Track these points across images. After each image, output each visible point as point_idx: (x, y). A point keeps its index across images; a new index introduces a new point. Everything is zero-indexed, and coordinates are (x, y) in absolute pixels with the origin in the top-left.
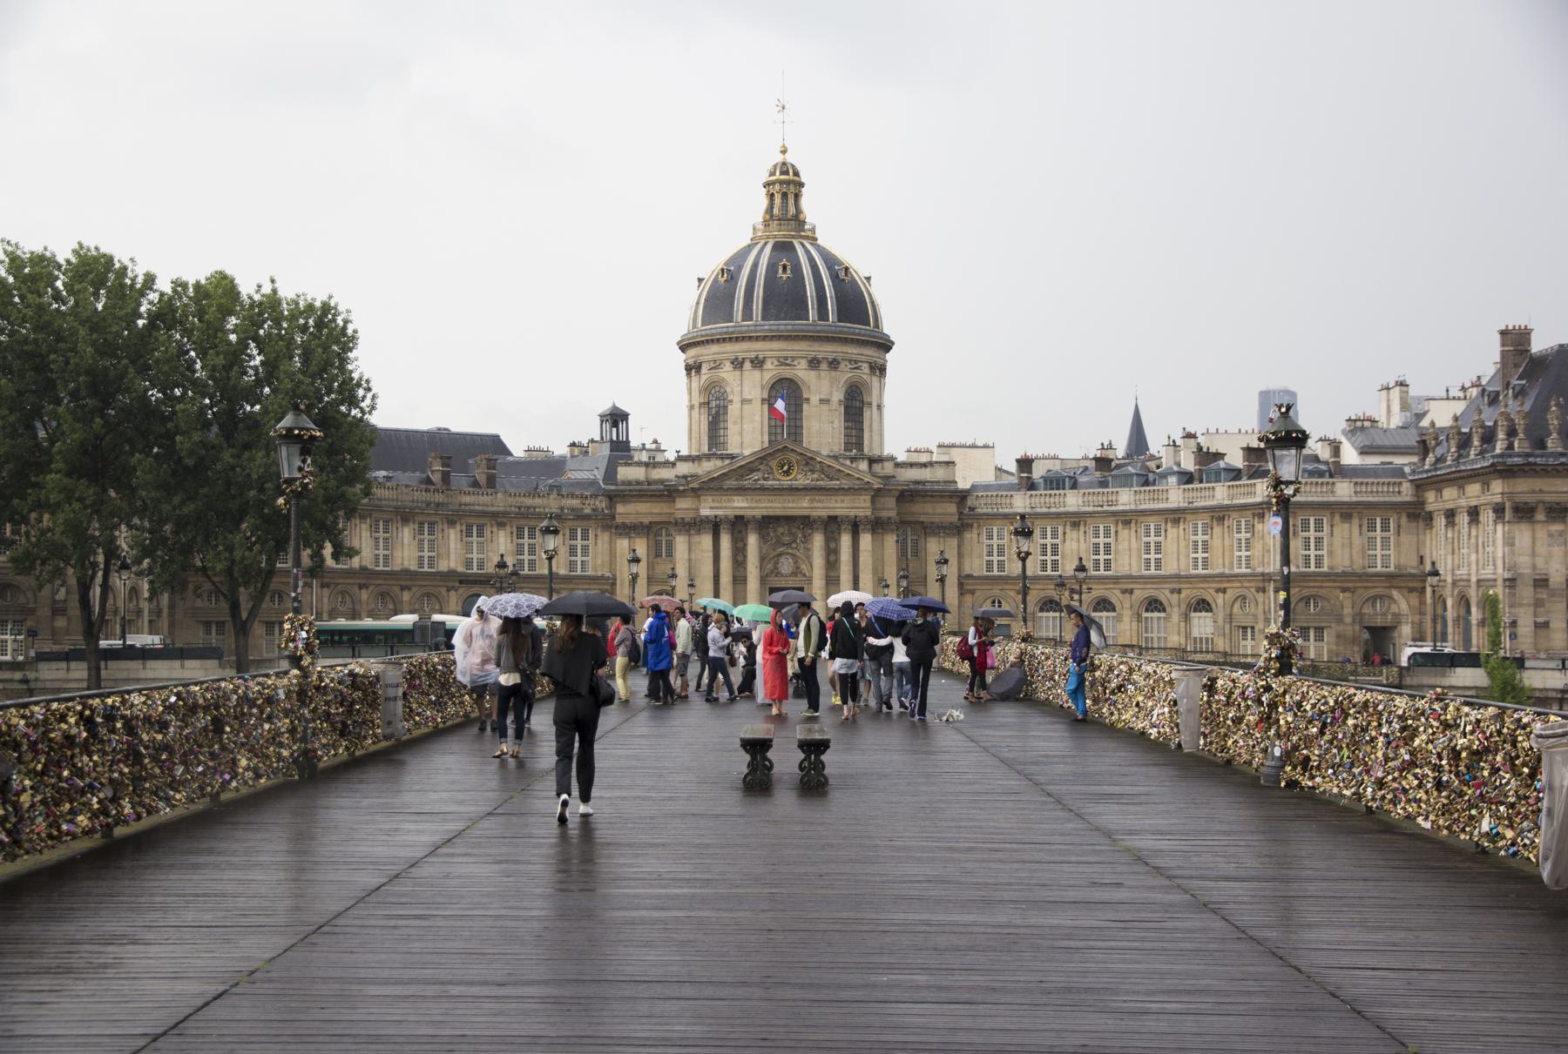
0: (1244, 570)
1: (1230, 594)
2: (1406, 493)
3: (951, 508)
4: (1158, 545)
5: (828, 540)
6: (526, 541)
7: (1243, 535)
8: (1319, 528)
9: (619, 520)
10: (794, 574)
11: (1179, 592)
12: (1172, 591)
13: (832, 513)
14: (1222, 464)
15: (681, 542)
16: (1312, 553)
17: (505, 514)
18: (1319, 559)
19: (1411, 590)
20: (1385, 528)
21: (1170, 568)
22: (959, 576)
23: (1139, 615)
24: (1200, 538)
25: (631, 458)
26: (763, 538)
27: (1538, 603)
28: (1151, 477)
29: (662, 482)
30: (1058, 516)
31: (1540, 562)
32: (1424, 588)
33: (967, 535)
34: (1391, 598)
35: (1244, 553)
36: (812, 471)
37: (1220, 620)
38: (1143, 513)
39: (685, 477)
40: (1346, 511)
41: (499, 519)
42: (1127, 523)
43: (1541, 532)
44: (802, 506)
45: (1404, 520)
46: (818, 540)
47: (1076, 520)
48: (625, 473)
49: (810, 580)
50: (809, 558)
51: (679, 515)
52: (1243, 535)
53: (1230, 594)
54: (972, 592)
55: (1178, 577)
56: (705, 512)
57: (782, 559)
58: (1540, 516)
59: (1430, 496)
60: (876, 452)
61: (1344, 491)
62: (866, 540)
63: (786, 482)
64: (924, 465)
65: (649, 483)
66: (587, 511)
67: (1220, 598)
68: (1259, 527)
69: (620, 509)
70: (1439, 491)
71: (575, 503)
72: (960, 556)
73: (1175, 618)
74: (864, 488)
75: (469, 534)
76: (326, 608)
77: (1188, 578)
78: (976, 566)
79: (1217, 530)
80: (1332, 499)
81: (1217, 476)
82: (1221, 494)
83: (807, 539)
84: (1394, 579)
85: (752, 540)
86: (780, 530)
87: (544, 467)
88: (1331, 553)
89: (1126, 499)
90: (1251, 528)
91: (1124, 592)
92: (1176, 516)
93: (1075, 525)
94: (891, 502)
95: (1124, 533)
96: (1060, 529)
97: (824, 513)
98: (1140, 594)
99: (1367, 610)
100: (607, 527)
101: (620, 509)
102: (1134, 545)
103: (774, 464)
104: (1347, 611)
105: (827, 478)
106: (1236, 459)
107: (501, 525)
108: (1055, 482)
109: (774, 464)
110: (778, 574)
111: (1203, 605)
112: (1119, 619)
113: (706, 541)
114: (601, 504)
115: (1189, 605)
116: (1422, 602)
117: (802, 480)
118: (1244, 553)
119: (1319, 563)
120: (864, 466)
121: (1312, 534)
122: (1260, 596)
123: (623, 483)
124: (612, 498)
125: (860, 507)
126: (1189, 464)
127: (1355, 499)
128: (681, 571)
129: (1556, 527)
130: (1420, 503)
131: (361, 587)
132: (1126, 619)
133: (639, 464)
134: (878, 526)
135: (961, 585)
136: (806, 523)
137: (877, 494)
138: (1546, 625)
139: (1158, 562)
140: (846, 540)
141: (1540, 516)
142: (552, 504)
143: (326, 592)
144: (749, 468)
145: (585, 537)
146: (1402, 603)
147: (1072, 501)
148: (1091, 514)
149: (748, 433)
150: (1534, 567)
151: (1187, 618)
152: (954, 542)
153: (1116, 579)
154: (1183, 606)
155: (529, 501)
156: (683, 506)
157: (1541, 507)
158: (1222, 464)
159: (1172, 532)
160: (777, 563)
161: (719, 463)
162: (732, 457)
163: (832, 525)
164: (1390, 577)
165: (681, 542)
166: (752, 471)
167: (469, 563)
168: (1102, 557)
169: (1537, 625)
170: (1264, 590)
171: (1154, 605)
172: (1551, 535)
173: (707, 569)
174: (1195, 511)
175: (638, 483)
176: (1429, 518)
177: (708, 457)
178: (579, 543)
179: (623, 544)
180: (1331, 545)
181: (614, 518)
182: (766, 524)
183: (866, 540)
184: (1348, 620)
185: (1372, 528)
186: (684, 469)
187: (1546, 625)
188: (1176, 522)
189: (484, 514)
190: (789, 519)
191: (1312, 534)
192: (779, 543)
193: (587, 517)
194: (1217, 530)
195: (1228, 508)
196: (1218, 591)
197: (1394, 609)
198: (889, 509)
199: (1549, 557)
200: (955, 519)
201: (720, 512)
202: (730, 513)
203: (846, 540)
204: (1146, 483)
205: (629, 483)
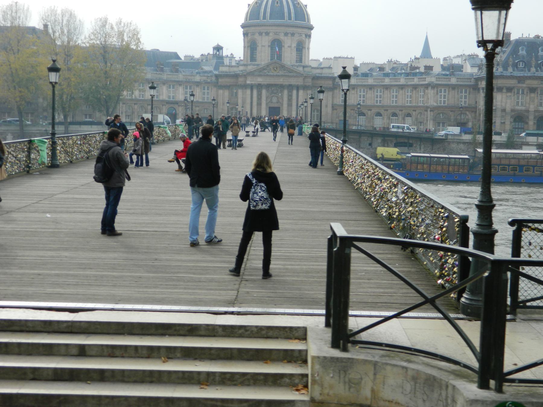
0: (421, 104)
1: (417, 112)
2: (472, 82)
3: (330, 82)
4: (396, 96)
5: (289, 92)
7: (422, 94)
8: (445, 92)
9: (219, 84)
10: (277, 103)
11: (402, 111)
12: (400, 110)
13: (290, 83)
14: (418, 71)
15: (240, 92)
16: (442, 99)
17: (182, 81)
18: (444, 102)
19: (472, 112)
20: (466, 92)
21: (400, 103)
22: (332, 104)
23: (389, 118)
24: (409, 94)
25: (223, 63)
26: (268, 91)
27: (502, 116)
28: (396, 74)
29: (234, 72)
30: (365, 86)
31: (503, 104)
32: (476, 111)
33: (335, 91)
34: (466, 114)
35: (422, 99)
36: (284, 70)
37: (414, 119)
38: (392, 86)
39: (242, 71)
40: (453, 87)
41: (180, 83)
42: (387, 89)
43: (504, 96)
44: (280, 81)
45: (471, 90)
46: (286, 92)
47: (371, 87)
48: (222, 69)
49: (282, 105)
50: (282, 97)
51: (239, 83)
52: (422, 94)
53: (417, 112)
54: (336, 109)
55: (402, 107)
56: (248, 82)
57: (273, 98)
58: (504, 91)
59: (479, 83)
60: (307, 64)
61: (453, 81)
62: (301, 92)
63: (275, 73)
64: (322, 68)
65: (230, 72)
66: (209, 81)
67: (414, 113)
68: (426, 91)
69: (220, 80)
70: (481, 81)
71: (205, 78)
72: (333, 98)
73: (400, 119)
74: (302, 75)
75: (170, 88)
76: (124, 110)
77: (405, 107)
79: (414, 92)
80: (449, 83)
81: (415, 74)
82: (416, 81)
83: (282, 92)
84: (466, 108)
85: (264, 92)
86: (273, 89)
87: (193, 64)
88: (448, 100)
89: (387, 81)
90: (424, 92)
91: (385, 110)
92: (402, 87)
93: (370, 89)
94: (310, 80)
95: (386, 92)
96: (366, 90)
97: (287, 83)
98: (390, 111)
99: (459, 117)
100: (215, 86)
101: (220, 80)
102: (389, 96)
103: (271, 67)
104: (452, 118)
105: (289, 71)
106: (422, 70)
107: (180, 85)
108: (365, 75)
109: (271, 67)
110: (272, 103)
111: (409, 115)
112: (383, 119)
113: (248, 92)
114: (214, 79)
115: (405, 115)
116: (476, 116)
117: (281, 73)
118: (422, 99)
119: (444, 103)
120: (301, 69)
121: (443, 94)
122: (426, 113)
123: (221, 72)
124: (217, 76)
125: (299, 81)
126: (408, 71)
127: (456, 83)
128: (240, 102)
129: (509, 94)
130: (477, 85)
131: (135, 104)
132: (385, 119)
133: (226, 66)
134: (305, 88)
135: (333, 107)
136: (282, 87)
137: (306, 77)
138: (504, 123)
139: (396, 102)
140: (295, 92)
141: (504, 91)
142: (198, 78)
143: (124, 105)
144: (263, 69)
145: (208, 89)
146: (470, 116)
147: (370, 81)
148: (376, 85)
149: (264, 56)
150: (502, 105)
151: (404, 119)
152: (331, 93)
153: (383, 107)
154: (403, 115)
155: (189, 77)
156: (241, 80)
157: (505, 88)
158: (418, 71)
159: (401, 92)
160: (271, 99)
161: (253, 67)
162: (258, 65)
163: (290, 87)
164: (466, 107)
165: (240, 92)
166: (264, 69)
167: (169, 97)
168: (379, 99)
169: (501, 123)
170: (427, 111)
171: (394, 115)
172: (507, 96)
173: (248, 101)
174: (408, 86)
175: (226, 72)
176: (479, 89)
177: (250, 65)
178: (206, 91)
179: (221, 91)
180: (448, 97)
181: (217, 83)
183: (301, 92)
184: (452, 120)
185: (462, 92)
186: (241, 68)
187: (504, 123)
188: (402, 89)
189: (175, 81)
190: (276, 85)
191: (443, 94)
193: (209, 83)
194: (414, 92)
195: (418, 85)
196: (413, 110)
197: (467, 117)
198: (309, 82)
199: (506, 103)
200: (332, 86)
201: (253, 83)
202: (256, 83)
203: (295, 92)
204: (395, 76)
205: (223, 72)
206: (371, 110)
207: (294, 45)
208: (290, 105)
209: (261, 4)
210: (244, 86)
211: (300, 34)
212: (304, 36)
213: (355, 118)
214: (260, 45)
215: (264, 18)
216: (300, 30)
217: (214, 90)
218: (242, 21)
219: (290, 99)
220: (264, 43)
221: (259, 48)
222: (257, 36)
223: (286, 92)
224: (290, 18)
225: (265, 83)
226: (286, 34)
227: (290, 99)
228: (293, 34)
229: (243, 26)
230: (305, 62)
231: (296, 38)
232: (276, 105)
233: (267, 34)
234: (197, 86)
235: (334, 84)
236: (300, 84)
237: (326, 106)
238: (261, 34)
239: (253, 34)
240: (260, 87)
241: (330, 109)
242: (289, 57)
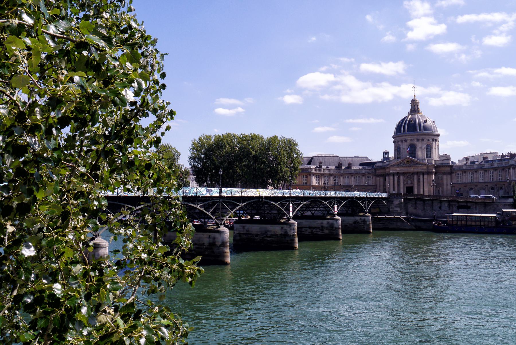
6: (358, 179)
21: (495, 180)
62: (426, 176)
78: (455, 181)
83: (413, 176)
89: (486, 166)
98: (489, 186)
101: (377, 171)
107: (352, 176)
113: (391, 178)
114: (374, 171)
140: (421, 177)
151: (498, 191)
152: (450, 176)
171: (493, 188)
173: (392, 183)
179: (378, 178)
182: (403, 174)
183: (426, 176)
190: (409, 173)
192: (408, 177)
193: (370, 173)
203: (421, 177)
206: (477, 186)
207: (424, 146)
208: (419, 184)
209: (402, 123)
210: (389, 174)
211: (428, 140)
212: (431, 140)
213: (468, 192)
214: (402, 148)
215: (404, 131)
216: (428, 137)
217: (374, 178)
218: (393, 134)
219: (419, 181)
220: (404, 146)
221: (402, 150)
222: (400, 143)
223: (416, 177)
224: (420, 130)
225: (402, 171)
226: (418, 140)
227: (419, 181)
228: (423, 140)
229: (393, 138)
230: (435, 157)
231: (425, 141)
232: (411, 185)
233: (406, 141)
234: (363, 176)
235: (451, 170)
236: (424, 171)
237: (447, 185)
238: (402, 141)
239: (398, 142)
240: (398, 174)
241: (449, 187)
242: (421, 154)
